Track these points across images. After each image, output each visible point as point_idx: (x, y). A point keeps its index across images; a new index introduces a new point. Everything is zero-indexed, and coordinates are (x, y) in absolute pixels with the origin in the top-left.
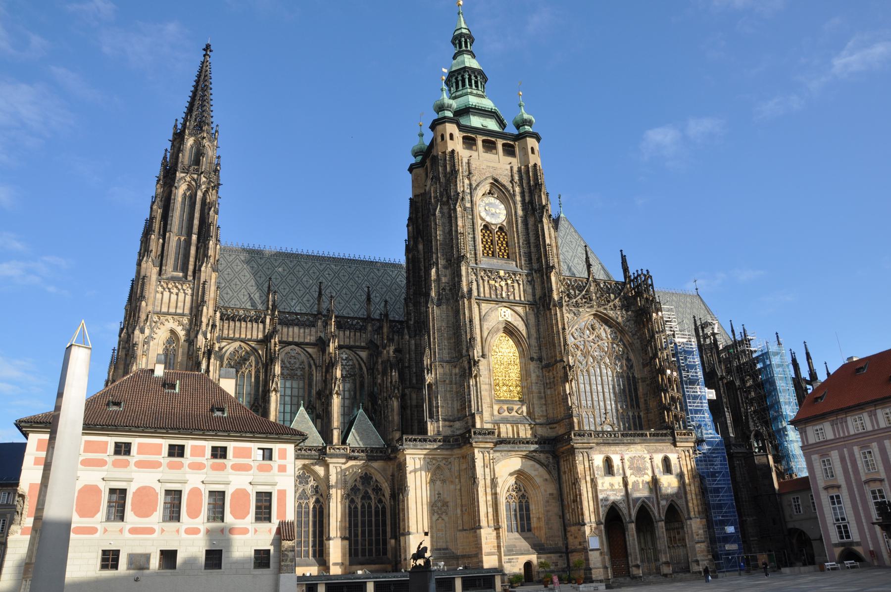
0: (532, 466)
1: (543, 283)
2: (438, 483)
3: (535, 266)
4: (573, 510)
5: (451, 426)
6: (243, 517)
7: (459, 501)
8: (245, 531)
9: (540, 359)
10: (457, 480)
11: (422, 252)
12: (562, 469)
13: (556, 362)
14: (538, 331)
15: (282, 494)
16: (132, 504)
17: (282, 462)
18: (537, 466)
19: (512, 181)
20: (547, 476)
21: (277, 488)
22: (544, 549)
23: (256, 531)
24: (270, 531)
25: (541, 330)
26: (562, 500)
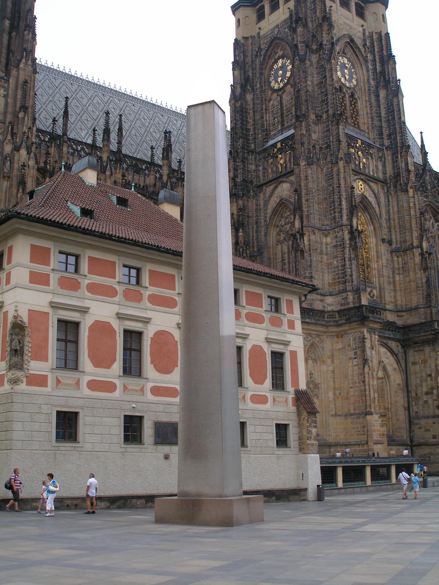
0: (385, 353)
1: (395, 161)
2: (310, 361)
3: (387, 142)
4: (426, 402)
5: (322, 301)
6: (262, 383)
7: (331, 383)
8: (262, 399)
9: (390, 243)
10: (330, 360)
11: (250, 102)
12: (411, 359)
13: (411, 247)
14: (388, 212)
15: (294, 354)
16: (151, 355)
17: (289, 316)
18: (389, 354)
19: (365, 45)
20: (396, 366)
21: (291, 348)
22: (393, 441)
23: (274, 400)
24: (286, 401)
25: (391, 211)
26: (408, 392)
